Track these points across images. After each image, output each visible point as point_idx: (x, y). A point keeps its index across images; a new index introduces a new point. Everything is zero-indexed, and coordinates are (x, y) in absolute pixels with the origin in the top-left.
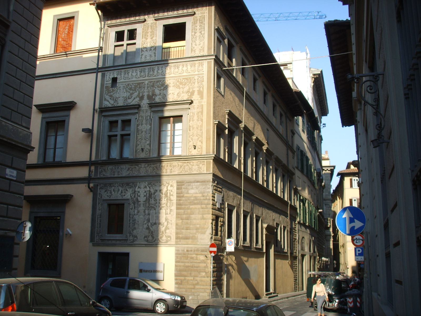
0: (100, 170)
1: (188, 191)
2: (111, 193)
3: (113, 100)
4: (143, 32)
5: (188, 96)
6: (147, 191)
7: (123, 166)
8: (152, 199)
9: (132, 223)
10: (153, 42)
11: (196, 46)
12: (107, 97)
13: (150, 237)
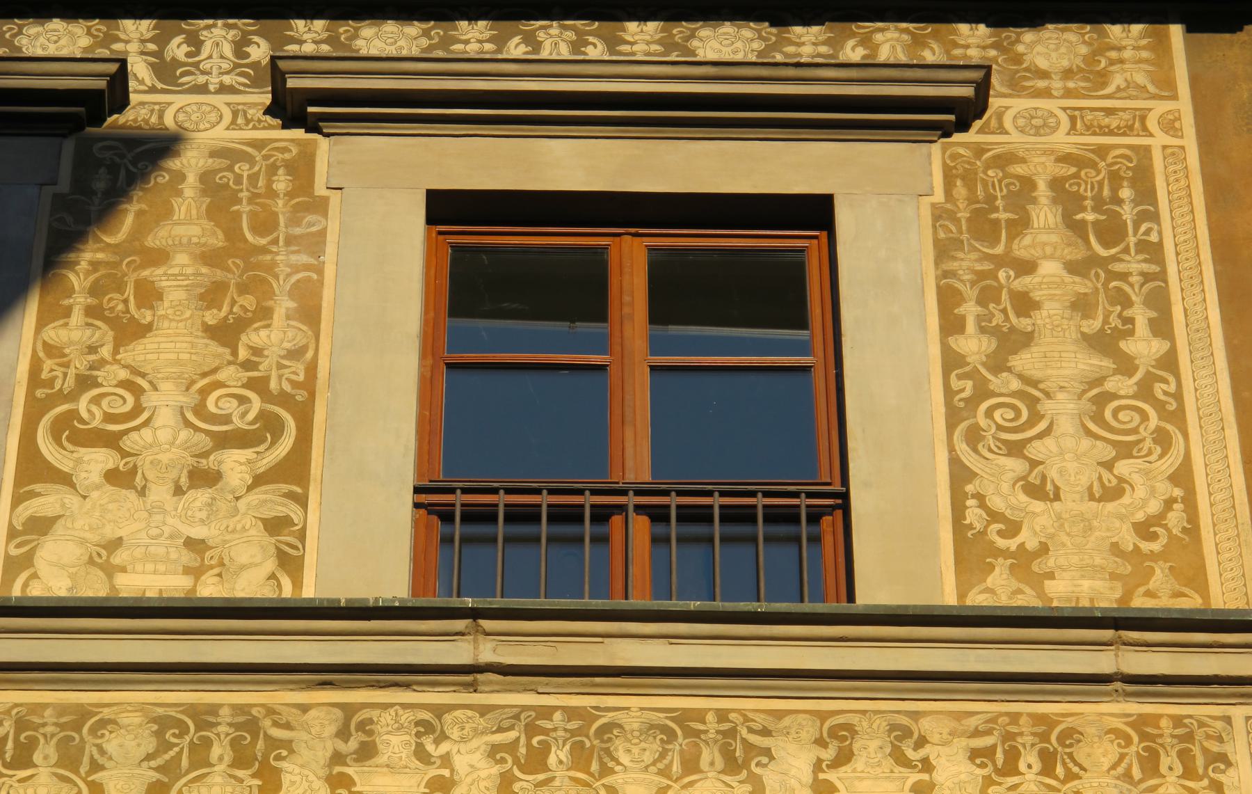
10: (258, 385)
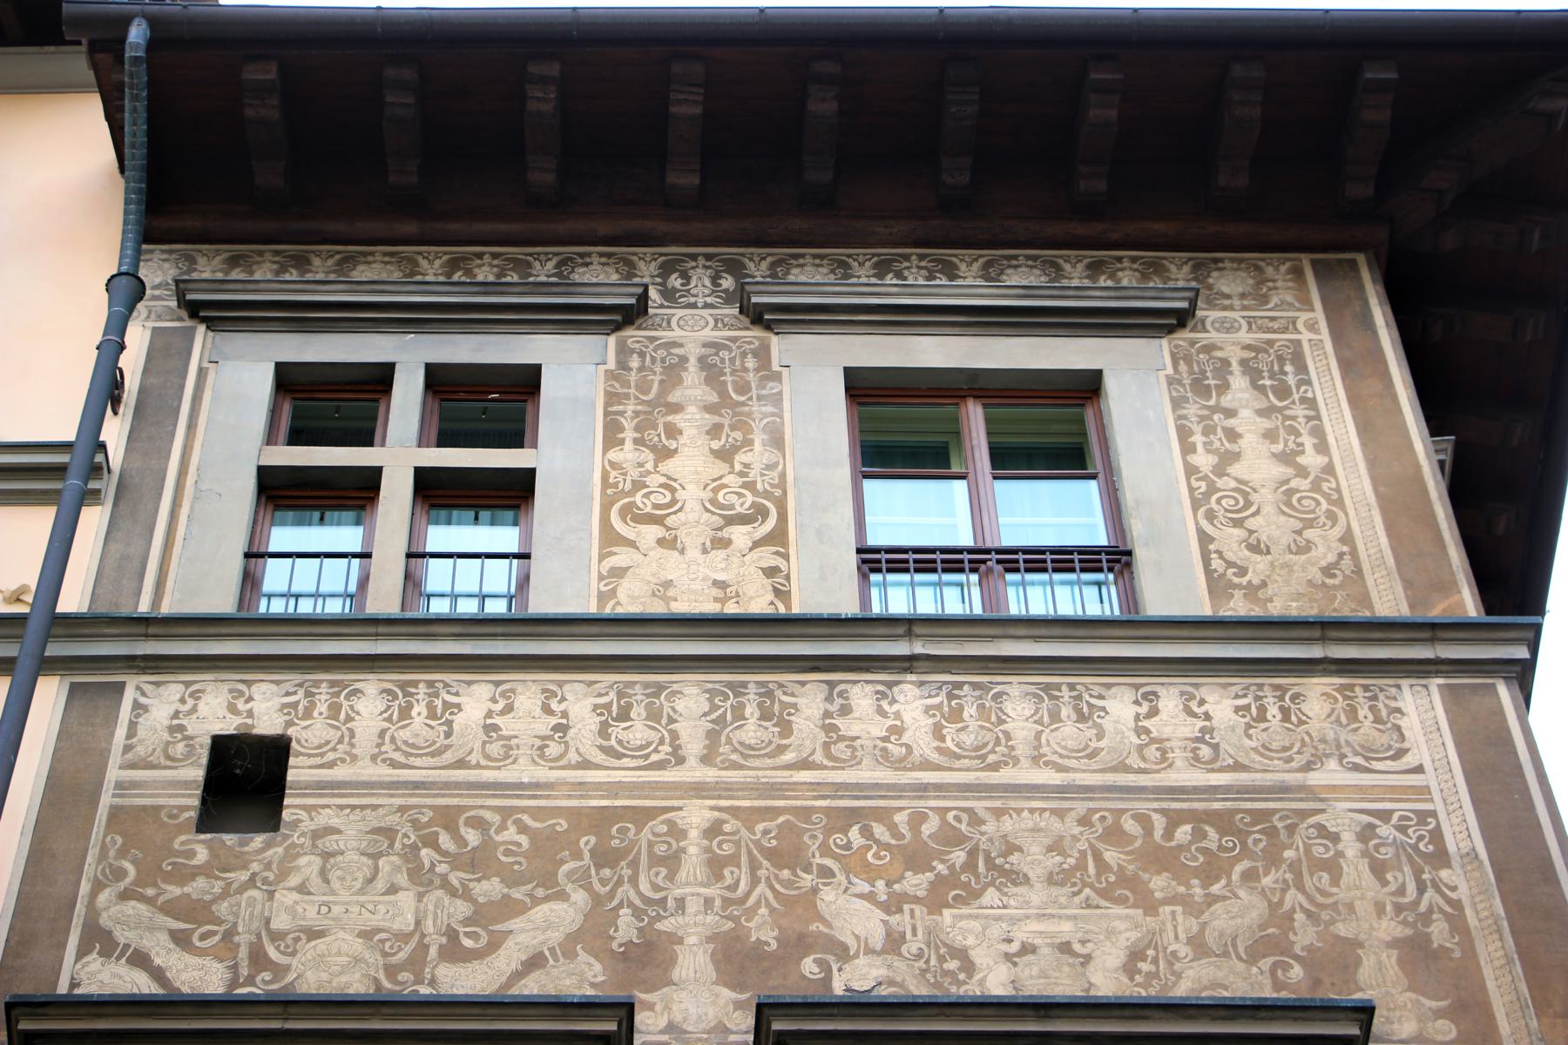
4: (611, 398)
10: (750, 486)
11: (1258, 558)
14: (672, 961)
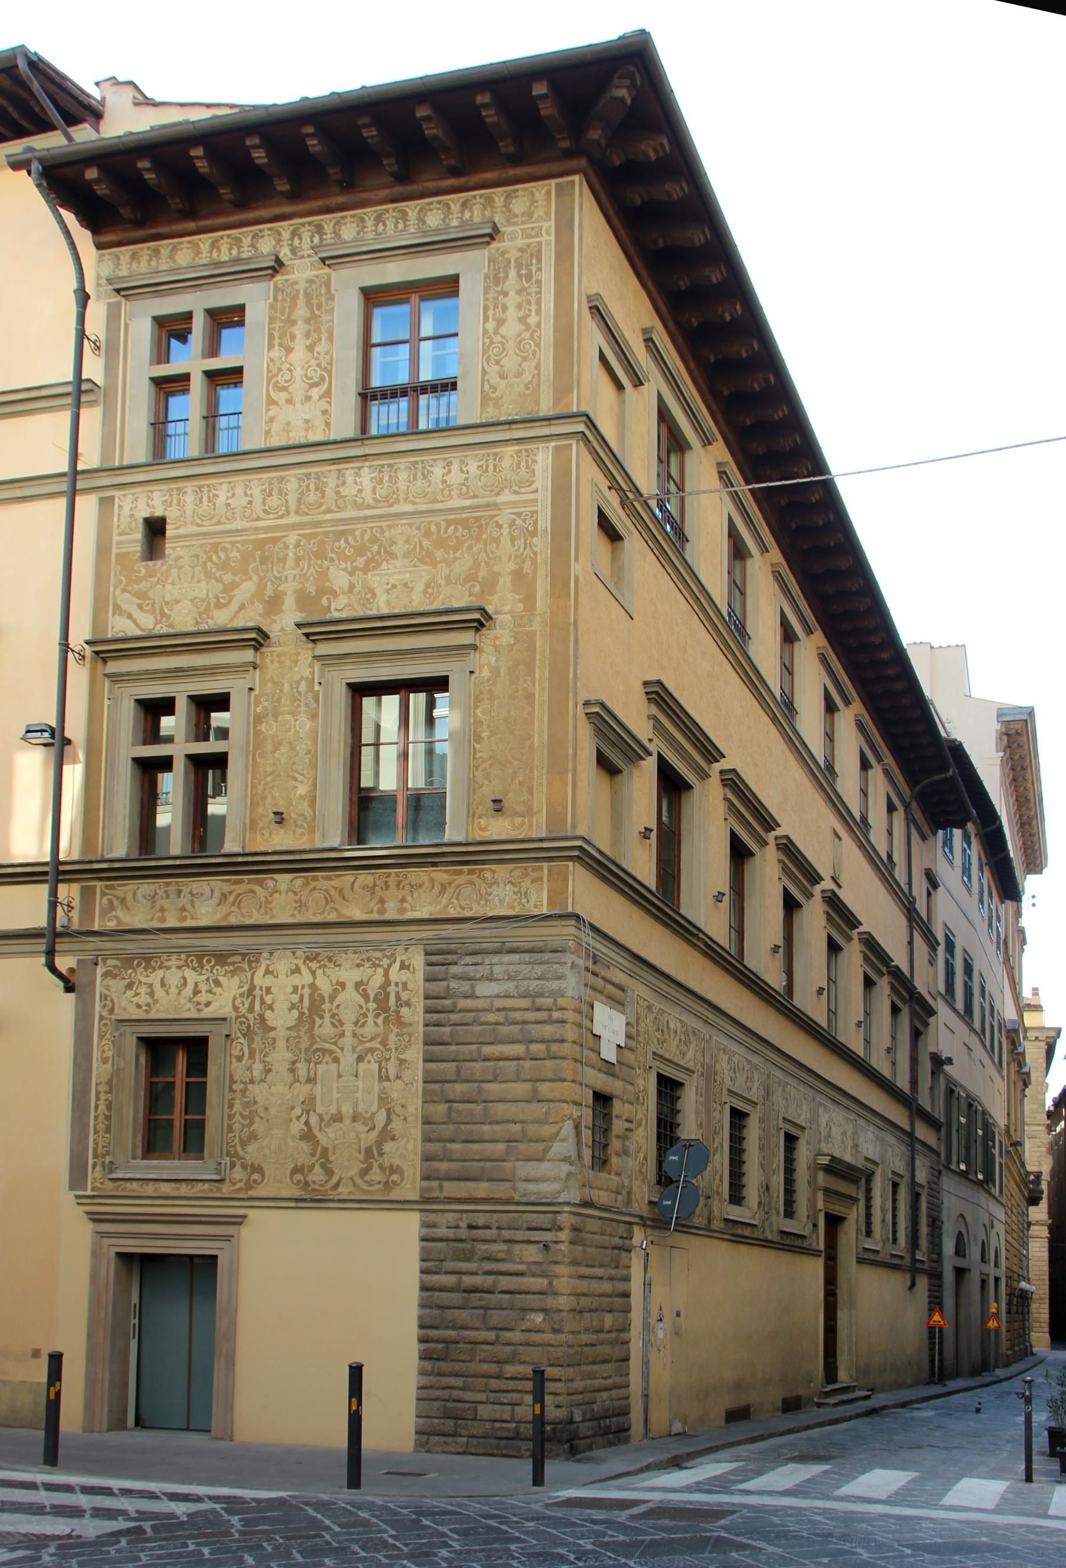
0: (105, 900)
1: (472, 987)
2: (152, 994)
3: (153, 610)
5: (471, 594)
6: (303, 987)
7: (201, 885)
8: (322, 1017)
9: (241, 1114)
12: (128, 602)
13: (317, 1169)
14: (283, 602)
